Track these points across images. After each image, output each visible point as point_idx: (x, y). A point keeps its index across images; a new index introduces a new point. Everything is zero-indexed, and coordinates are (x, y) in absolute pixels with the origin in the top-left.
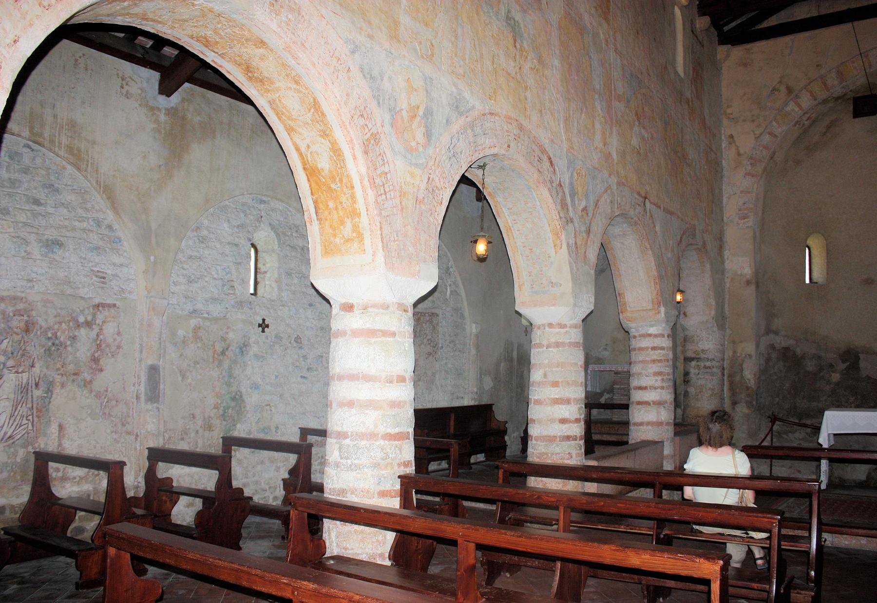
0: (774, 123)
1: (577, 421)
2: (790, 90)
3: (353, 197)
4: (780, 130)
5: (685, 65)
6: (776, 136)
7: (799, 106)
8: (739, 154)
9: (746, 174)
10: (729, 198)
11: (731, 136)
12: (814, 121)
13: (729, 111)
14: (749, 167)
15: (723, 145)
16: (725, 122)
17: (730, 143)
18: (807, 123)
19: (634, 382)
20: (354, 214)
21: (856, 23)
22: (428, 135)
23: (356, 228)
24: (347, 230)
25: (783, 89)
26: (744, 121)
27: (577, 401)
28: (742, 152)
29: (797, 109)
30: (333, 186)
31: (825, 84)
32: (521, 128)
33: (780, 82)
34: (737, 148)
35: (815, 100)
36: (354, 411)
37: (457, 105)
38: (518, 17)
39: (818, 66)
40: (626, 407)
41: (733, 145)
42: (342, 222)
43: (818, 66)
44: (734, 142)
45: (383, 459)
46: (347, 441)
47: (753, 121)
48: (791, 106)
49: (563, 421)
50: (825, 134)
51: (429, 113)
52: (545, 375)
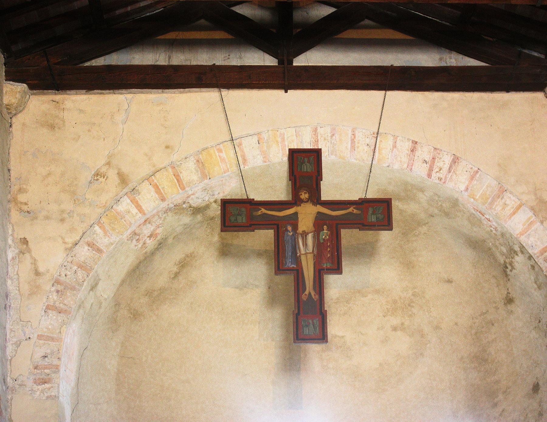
0: (97, 228)
2: (123, 179)
4: (106, 240)
6: (99, 251)
7: (139, 207)
8: (37, 273)
9: (48, 308)
10: (18, 344)
11: (25, 241)
12: (161, 245)
13: (22, 198)
14: (55, 296)
15: (10, 255)
16: (15, 215)
17: (22, 252)
18: (151, 244)
21: (225, 92)
25: (112, 174)
26: (47, 218)
28: (41, 269)
29: (134, 211)
31: (177, 176)
33: (108, 164)
34: (34, 262)
35: (163, 200)
39: (167, 147)
41: (27, 255)
43: (167, 147)
44: (29, 251)
47: (62, 220)
50: (177, 275)
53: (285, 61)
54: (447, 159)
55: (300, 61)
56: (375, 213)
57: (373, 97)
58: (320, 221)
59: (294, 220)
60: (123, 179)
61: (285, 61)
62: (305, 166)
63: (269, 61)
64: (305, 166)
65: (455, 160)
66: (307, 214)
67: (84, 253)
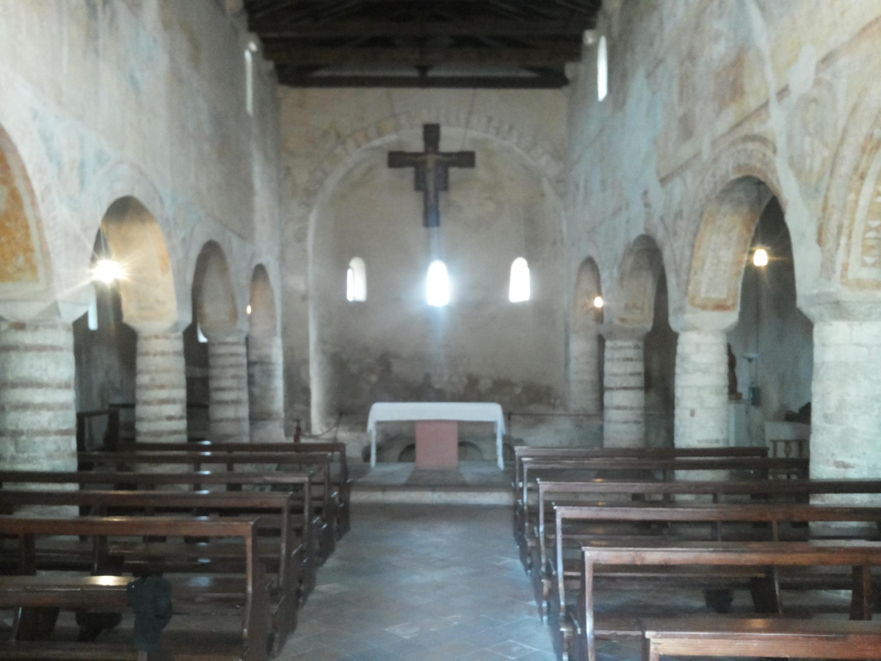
1: (181, 418)
2: (338, 136)
3: (27, 236)
5: (254, 103)
19: (213, 384)
20: (28, 250)
22: (82, 183)
23: (28, 260)
24: (20, 261)
27: (181, 401)
30: (7, 224)
32: (141, 173)
36: (29, 413)
37: (101, 159)
38: (138, 75)
40: (206, 407)
42: (14, 254)
45: (56, 451)
46: (24, 438)
48: (339, 150)
49: (170, 418)
51: (82, 165)
52: (153, 380)
53: (423, 69)
54: (506, 127)
55: (431, 73)
56: (466, 159)
57: (468, 92)
58: (438, 163)
59: (424, 163)
60: (338, 136)
61: (423, 69)
62: (431, 133)
63: (415, 73)
64: (431, 133)
65: (511, 128)
66: (431, 160)
67: (319, 174)
